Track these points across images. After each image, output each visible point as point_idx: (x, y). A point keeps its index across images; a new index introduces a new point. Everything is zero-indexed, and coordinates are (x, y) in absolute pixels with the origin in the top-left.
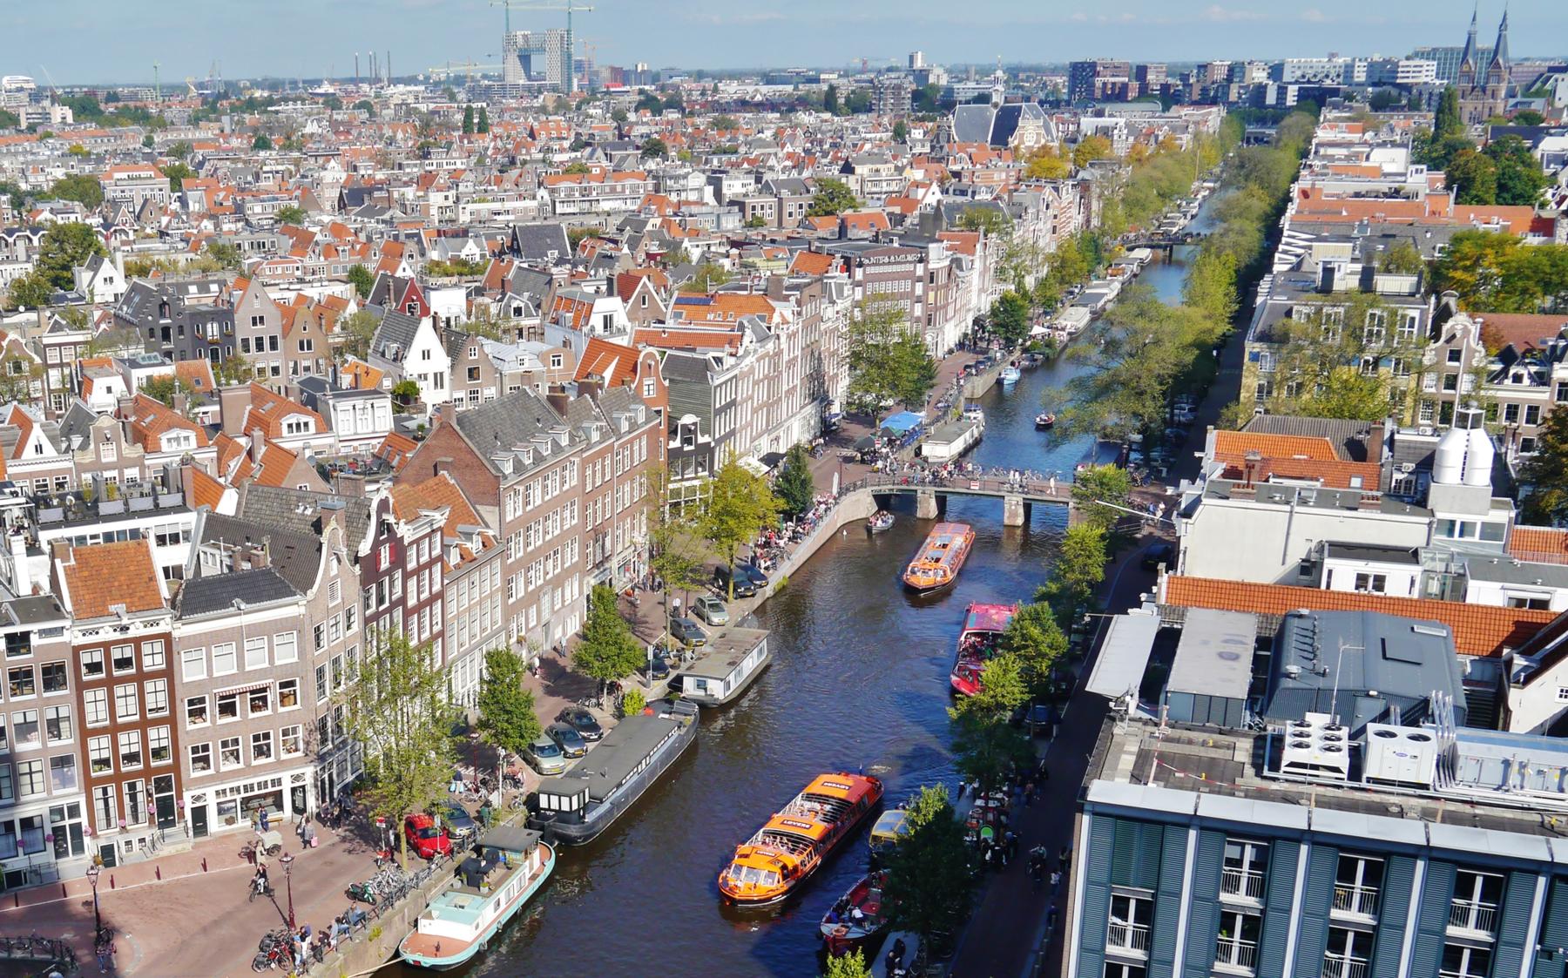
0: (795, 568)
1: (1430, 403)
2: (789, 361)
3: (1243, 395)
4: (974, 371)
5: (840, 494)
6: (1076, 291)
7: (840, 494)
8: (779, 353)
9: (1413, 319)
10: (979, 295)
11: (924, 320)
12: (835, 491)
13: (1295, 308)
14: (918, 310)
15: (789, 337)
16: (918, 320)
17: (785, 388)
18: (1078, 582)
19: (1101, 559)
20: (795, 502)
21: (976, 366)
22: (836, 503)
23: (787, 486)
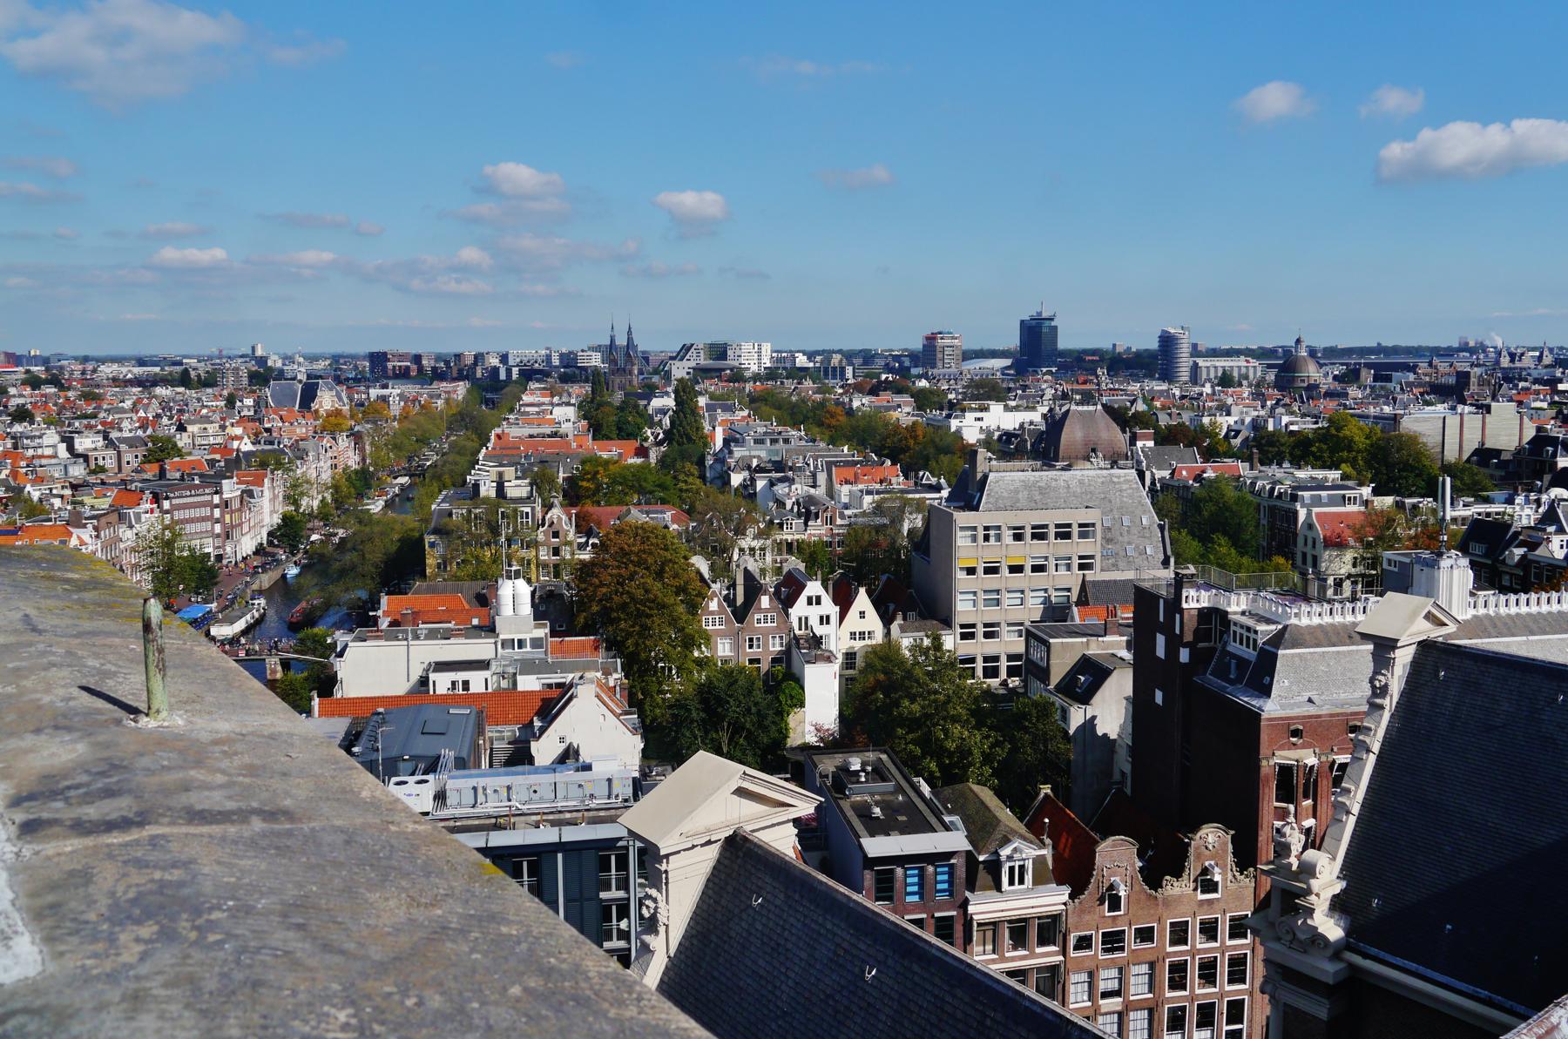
1: (545, 565)
3: (428, 571)
9: (527, 513)
13: (454, 511)
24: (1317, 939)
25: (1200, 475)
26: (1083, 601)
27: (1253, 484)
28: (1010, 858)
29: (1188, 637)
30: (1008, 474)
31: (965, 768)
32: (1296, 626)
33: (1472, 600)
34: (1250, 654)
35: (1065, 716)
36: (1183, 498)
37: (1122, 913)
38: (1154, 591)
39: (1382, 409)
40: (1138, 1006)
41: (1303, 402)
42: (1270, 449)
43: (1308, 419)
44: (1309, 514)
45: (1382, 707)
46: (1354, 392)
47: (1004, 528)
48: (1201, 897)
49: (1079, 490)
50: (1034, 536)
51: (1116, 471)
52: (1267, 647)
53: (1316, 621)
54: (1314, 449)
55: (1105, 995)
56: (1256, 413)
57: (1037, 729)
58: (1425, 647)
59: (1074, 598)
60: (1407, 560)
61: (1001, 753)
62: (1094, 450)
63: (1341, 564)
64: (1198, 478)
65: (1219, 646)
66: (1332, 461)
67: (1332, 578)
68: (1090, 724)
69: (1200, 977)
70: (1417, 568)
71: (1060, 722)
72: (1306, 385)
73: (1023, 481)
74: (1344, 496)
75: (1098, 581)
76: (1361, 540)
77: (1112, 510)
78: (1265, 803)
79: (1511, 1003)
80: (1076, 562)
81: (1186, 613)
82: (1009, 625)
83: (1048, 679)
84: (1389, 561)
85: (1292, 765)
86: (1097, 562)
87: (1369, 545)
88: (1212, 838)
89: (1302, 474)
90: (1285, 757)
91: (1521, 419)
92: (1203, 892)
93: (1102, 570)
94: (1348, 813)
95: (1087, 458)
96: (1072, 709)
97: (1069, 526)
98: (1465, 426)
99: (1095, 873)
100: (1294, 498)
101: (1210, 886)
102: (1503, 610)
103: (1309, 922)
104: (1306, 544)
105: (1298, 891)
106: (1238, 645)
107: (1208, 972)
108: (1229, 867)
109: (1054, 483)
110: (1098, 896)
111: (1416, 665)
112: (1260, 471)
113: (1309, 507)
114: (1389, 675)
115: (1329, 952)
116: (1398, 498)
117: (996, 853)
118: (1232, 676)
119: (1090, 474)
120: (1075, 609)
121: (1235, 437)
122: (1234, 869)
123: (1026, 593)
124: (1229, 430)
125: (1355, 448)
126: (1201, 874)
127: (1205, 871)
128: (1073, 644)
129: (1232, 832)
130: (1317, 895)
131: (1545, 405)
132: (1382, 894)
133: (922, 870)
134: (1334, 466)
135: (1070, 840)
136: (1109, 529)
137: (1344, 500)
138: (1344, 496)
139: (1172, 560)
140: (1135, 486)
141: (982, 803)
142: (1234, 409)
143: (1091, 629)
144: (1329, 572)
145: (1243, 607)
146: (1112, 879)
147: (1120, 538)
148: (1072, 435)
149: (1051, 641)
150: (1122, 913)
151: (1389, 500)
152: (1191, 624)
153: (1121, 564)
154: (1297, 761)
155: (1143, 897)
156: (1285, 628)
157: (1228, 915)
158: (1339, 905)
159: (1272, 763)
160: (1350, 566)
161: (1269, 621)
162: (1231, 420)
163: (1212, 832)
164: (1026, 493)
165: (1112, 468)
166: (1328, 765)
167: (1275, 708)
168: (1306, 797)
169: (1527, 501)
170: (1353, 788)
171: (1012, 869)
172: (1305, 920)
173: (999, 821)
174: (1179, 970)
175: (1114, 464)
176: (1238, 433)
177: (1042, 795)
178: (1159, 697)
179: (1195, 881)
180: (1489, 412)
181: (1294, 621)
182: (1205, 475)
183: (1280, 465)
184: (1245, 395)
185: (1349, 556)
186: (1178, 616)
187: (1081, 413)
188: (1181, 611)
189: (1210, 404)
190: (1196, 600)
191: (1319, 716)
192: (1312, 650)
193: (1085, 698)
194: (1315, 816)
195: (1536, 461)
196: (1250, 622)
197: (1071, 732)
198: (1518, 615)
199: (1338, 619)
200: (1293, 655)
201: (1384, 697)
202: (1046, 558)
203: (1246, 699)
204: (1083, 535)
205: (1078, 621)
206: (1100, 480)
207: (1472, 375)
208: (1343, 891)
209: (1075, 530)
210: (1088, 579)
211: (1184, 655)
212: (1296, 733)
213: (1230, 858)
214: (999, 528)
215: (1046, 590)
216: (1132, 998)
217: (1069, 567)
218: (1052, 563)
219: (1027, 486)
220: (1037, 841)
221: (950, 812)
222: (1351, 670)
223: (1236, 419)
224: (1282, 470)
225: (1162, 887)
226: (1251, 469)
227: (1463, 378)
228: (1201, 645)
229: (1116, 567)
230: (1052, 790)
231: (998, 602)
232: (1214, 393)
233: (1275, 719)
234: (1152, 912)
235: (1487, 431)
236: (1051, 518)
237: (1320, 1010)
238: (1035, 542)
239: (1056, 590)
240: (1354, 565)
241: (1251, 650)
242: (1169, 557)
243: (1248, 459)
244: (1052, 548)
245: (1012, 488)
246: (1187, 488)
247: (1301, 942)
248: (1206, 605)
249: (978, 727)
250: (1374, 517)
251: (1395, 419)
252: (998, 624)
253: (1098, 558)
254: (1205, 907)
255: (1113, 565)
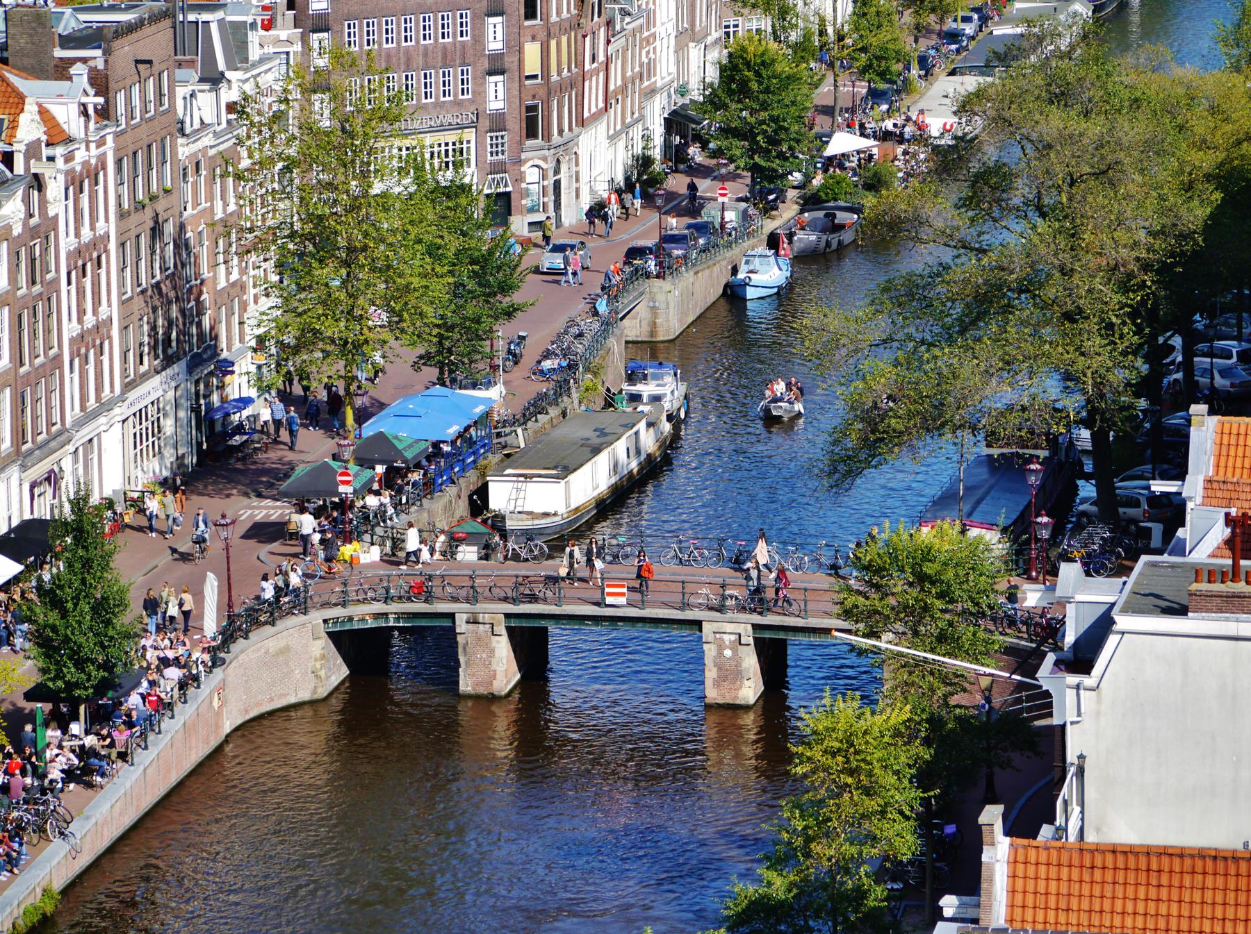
0: (84, 860)
2: (79, 252)
4: (652, 265)
5: (230, 633)
6: (969, 29)
7: (230, 633)
8: (43, 231)
10: (680, 49)
11: (515, 124)
12: (211, 624)
14: (496, 94)
15: (75, 183)
16: (498, 123)
17: (70, 329)
18: (844, 866)
19: (906, 796)
20: (80, 664)
21: (658, 252)
22: (216, 662)
23: (53, 617)
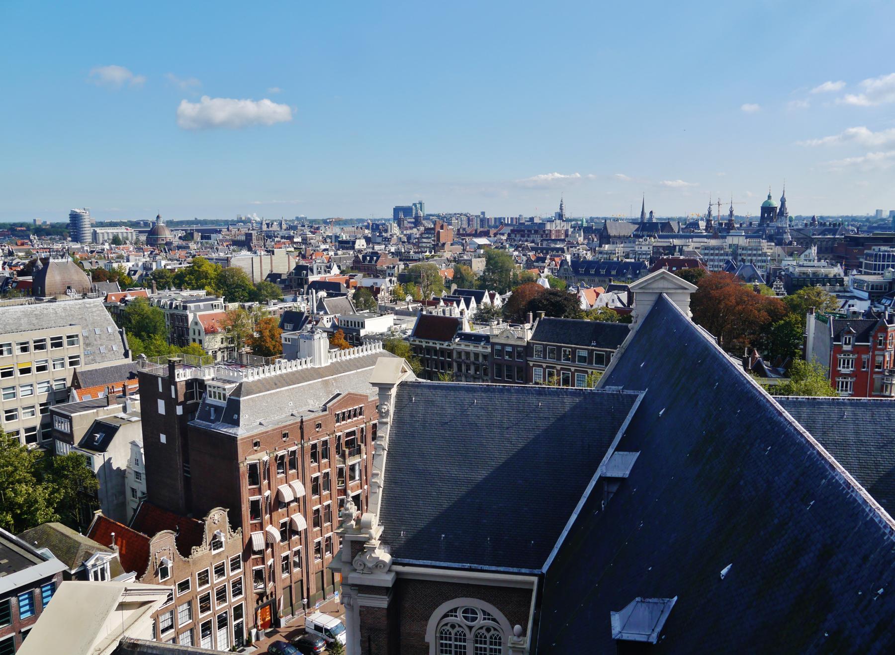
24: (379, 564)
25: (123, 299)
26: (76, 384)
27: (159, 302)
28: (94, 566)
29: (181, 399)
30: (11, 307)
31: (33, 514)
32: (247, 382)
33: (329, 355)
34: (223, 403)
35: (89, 461)
36: (115, 314)
37: (169, 577)
38: (154, 373)
39: (219, 255)
40: (183, 631)
41: (166, 252)
42: (161, 280)
43: (176, 262)
44: (195, 316)
45: (386, 423)
46: (193, 246)
47: (13, 345)
48: (214, 552)
49: (64, 314)
50: (36, 348)
51: (86, 300)
52: (232, 397)
53: (256, 378)
54: (187, 279)
55: (163, 631)
56: (145, 260)
57: (73, 475)
58: (403, 385)
59: (69, 384)
60: (297, 337)
61: (60, 496)
62: (69, 288)
63: (214, 343)
64: (123, 300)
65: (201, 401)
66: (197, 285)
67: (211, 351)
68: (108, 464)
69: (218, 599)
70: (302, 341)
71: (88, 467)
72: (165, 242)
73: (23, 311)
74: (212, 305)
75: (85, 372)
76: (224, 328)
77: (87, 325)
78: (244, 488)
79: (481, 566)
80: (67, 361)
81: (178, 384)
82: (24, 409)
83: (73, 440)
84: (286, 339)
85: (256, 463)
86: (82, 360)
87: (229, 331)
88: (217, 516)
89: (186, 293)
90: (252, 459)
91: (289, 257)
92: (214, 550)
93: (85, 364)
94: (379, 487)
95: (65, 293)
96: (95, 456)
97: (60, 338)
98: (263, 262)
99: (150, 558)
100: (185, 308)
101: (217, 544)
102: (344, 358)
103: (373, 555)
104: (194, 334)
105: (363, 540)
106: (213, 399)
107: (221, 595)
108: (228, 531)
109: (45, 312)
110: (154, 572)
111: (398, 396)
112: (158, 294)
113: (194, 312)
114: (389, 405)
115: (387, 569)
116: (241, 303)
117: (83, 565)
118: (212, 418)
119: (70, 303)
120: (74, 391)
121: (134, 274)
122: (231, 531)
123: (34, 386)
124: (130, 270)
125: (209, 277)
126: (213, 539)
127: (215, 537)
128: (87, 415)
129: (228, 510)
130: (375, 539)
131: (292, 249)
132: (405, 528)
133: (31, 593)
134: (201, 287)
135: (124, 541)
136: (87, 337)
137: (213, 307)
138: (212, 305)
139: (130, 352)
140: (101, 308)
141: (62, 534)
142: (131, 258)
143: (97, 403)
144: (210, 348)
145: (212, 376)
146: (162, 559)
147: (95, 343)
148: (53, 278)
149: (72, 415)
150: (169, 577)
151: (233, 306)
152: (182, 390)
153: (98, 359)
154: (259, 460)
155: (181, 563)
156: (241, 384)
157: (229, 558)
158: (384, 540)
159: (245, 464)
160: (220, 343)
161: (230, 382)
162: (130, 264)
163: (216, 513)
164: (26, 319)
165: (84, 298)
166: (274, 458)
167: (243, 432)
168: (264, 479)
169: (303, 300)
170: (379, 472)
171: (96, 573)
172: (371, 555)
173: (80, 543)
174: (205, 599)
175: (84, 296)
176: (136, 272)
177: (96, 517)
178: (163, 438)
179: (210, 544)
180: (273, 254)
181: (245, 380)
182: (126, 299)
183: (169, 289)
184: (131, 249)
185: (219, 338)
186: (173, 387)
187: (56, 264)
188: (175, 384)
189: (112, 255)
190: (183, 375)
191: (267, 432)
192: (258, 395)
193: (102, 447)
194: (269, 489)
195: (299, 278)
196: (220, 384)
197: (96, 471)
198: (350, 359)
199: (267, 375)
200: (248, 399)
201: (387, 418)
202: (46, 361)
203: (225, 430)
204: (72, 343)
205: (78, 401)
206: (77, 307)
207: (253, 235)
208: (384, 532)
209: (65, 341)
210: (78, 371)
211: (179, 410)
212: (256, 444)
213: (228, 525)
214: (10, 345)
215: (48, 382)
216: (180, 627)
217: (63, 365)
218: (51, 363)
219: (26, 314)
220: (109, 549)
221: (38, 547)
222: (279, 403)
223: (133, 263)
224: (172, 292)
225: (191, 554)
226: (153, 293)
227: (249, 236)
228: (189, 402)
229: (94, 361)
230: (102, 512)
231: (14, 395)
232: (111, 249)
233: (245, 438)
234: (187, 571)
235: (273, 264)
236: (47, 335)
237: (382, 602)
238: (37, 351)
239: (55, 381)
240: (222, 343)
241: (222, 401)
242: (128, 351)
243: (150, 287)
244: (49, 354)
245: (15, 317)
246: (116, 307)
247: (370, 568)
248: (190, 377)
249: (39, 481)
250: (231, 315)
251: (227, 260)
252: (16, 410)
253: (82, 356)
254: (217, 558)
255: (93, 360)
